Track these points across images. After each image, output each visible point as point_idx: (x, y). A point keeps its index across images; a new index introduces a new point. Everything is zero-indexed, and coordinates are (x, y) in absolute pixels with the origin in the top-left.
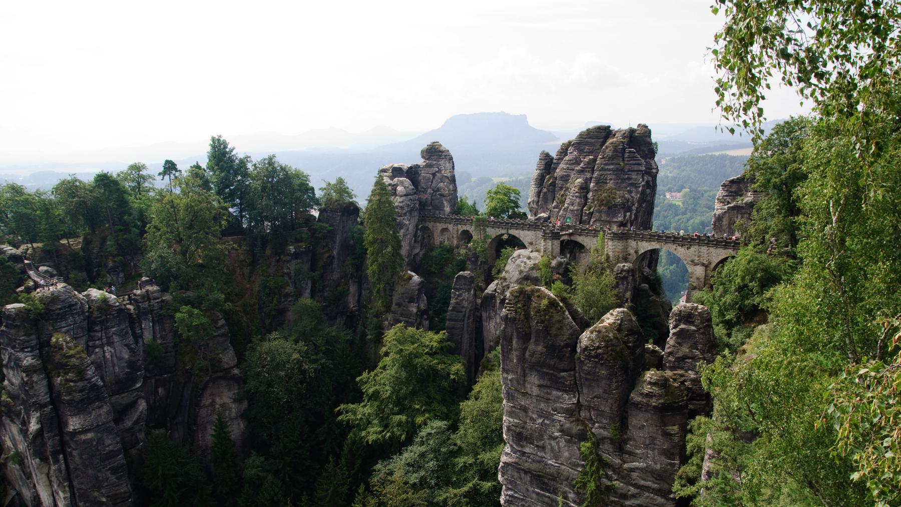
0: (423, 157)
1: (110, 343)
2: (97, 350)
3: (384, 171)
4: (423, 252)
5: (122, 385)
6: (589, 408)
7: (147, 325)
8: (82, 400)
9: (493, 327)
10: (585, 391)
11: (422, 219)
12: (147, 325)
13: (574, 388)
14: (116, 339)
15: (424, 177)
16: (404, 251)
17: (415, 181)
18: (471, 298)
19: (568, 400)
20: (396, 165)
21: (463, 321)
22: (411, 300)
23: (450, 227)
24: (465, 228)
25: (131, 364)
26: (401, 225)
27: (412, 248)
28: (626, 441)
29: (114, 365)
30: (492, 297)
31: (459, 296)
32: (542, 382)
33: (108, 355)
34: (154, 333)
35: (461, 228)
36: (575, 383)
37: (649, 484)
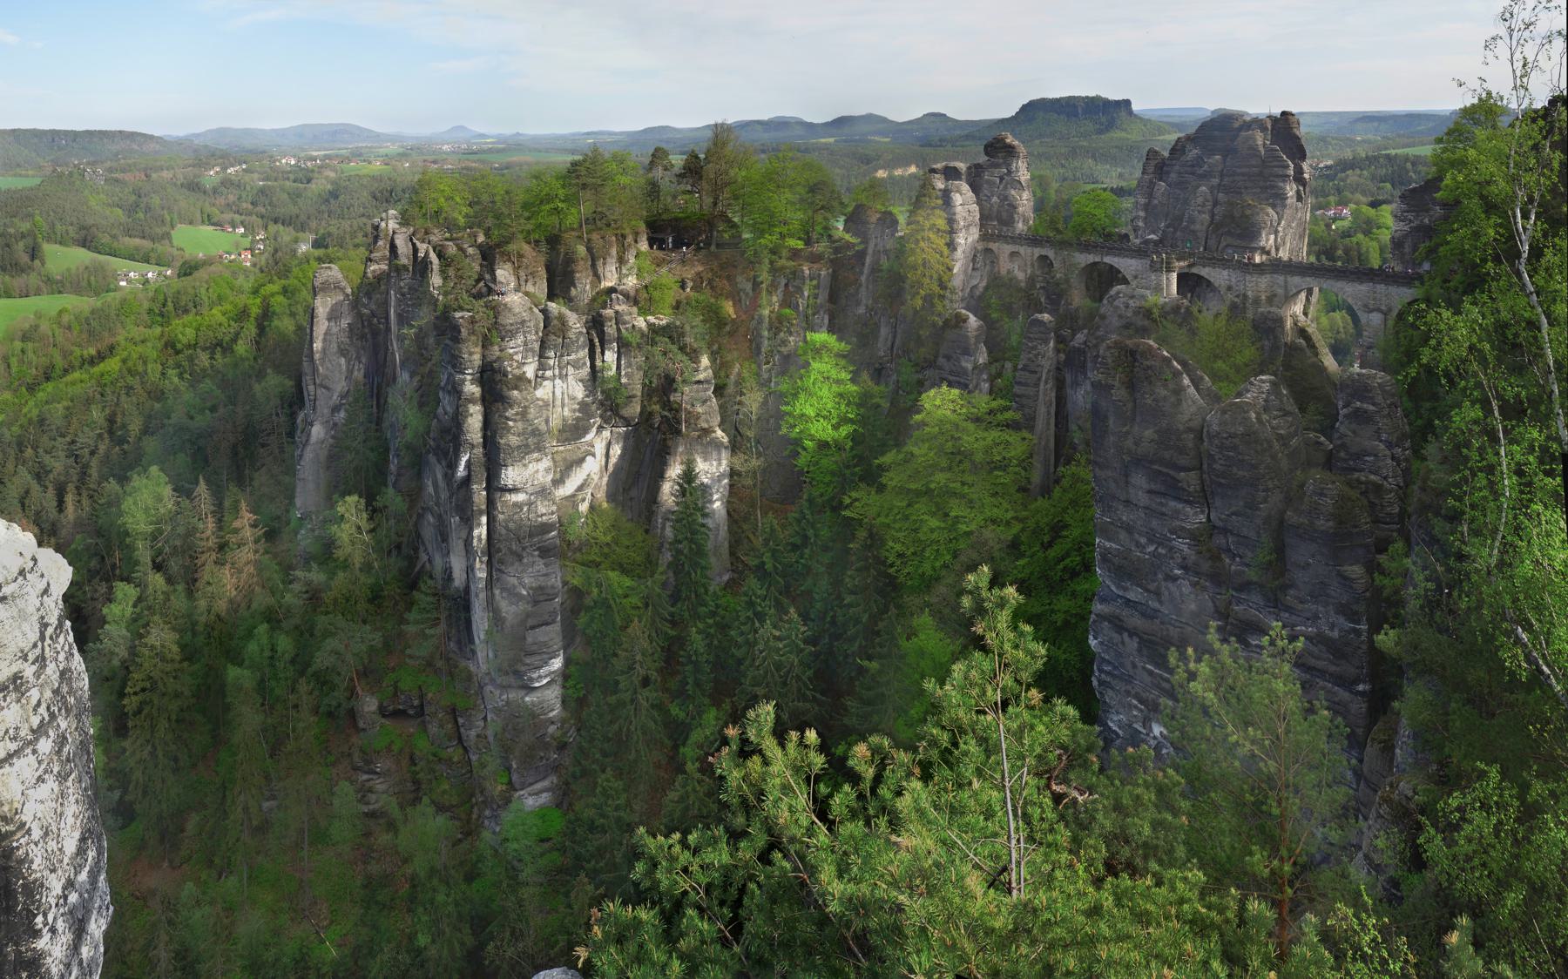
0: (987, 153)
1: (563, 377)
2: (546, 383)
3: (934, 171)
4: (984, 284)
5: (573, 431)
6: (1225, 531)
7: (610, 356)
8: (519, 447)
9: (1081, 397)
10: (1218, 502)
11: (984, 237)
12: (610, 356)
13: (1204, 498)
14: (571, 370)
15: (988, 182)
16: (957, 282)
17: (975, 188)
18: (1051, 353)
19: (1195, 518)
20: (952, 164)
21: (1037, 385)
22: (966, 352)
23: (1022, 250)
24: (1044, 252)
25: (583, 407)
26: (952, 246)
27: (969, 278)
28: (1284, 588)
29: (563, 406)
30: (1081, 352)
31: (1034, 348)
32: (1153, 487)
33: (558, 393)
34: (619, 368)
35: (1038, 252)
36: (1203, 490)
37: (1320, 664)
